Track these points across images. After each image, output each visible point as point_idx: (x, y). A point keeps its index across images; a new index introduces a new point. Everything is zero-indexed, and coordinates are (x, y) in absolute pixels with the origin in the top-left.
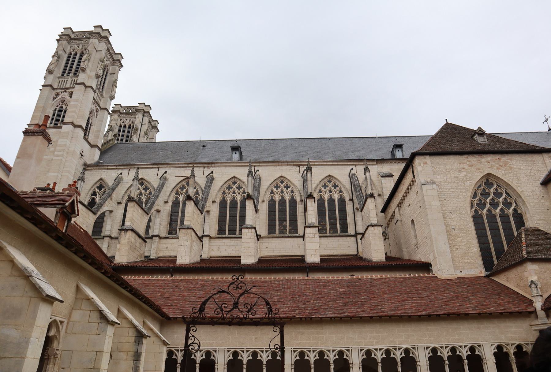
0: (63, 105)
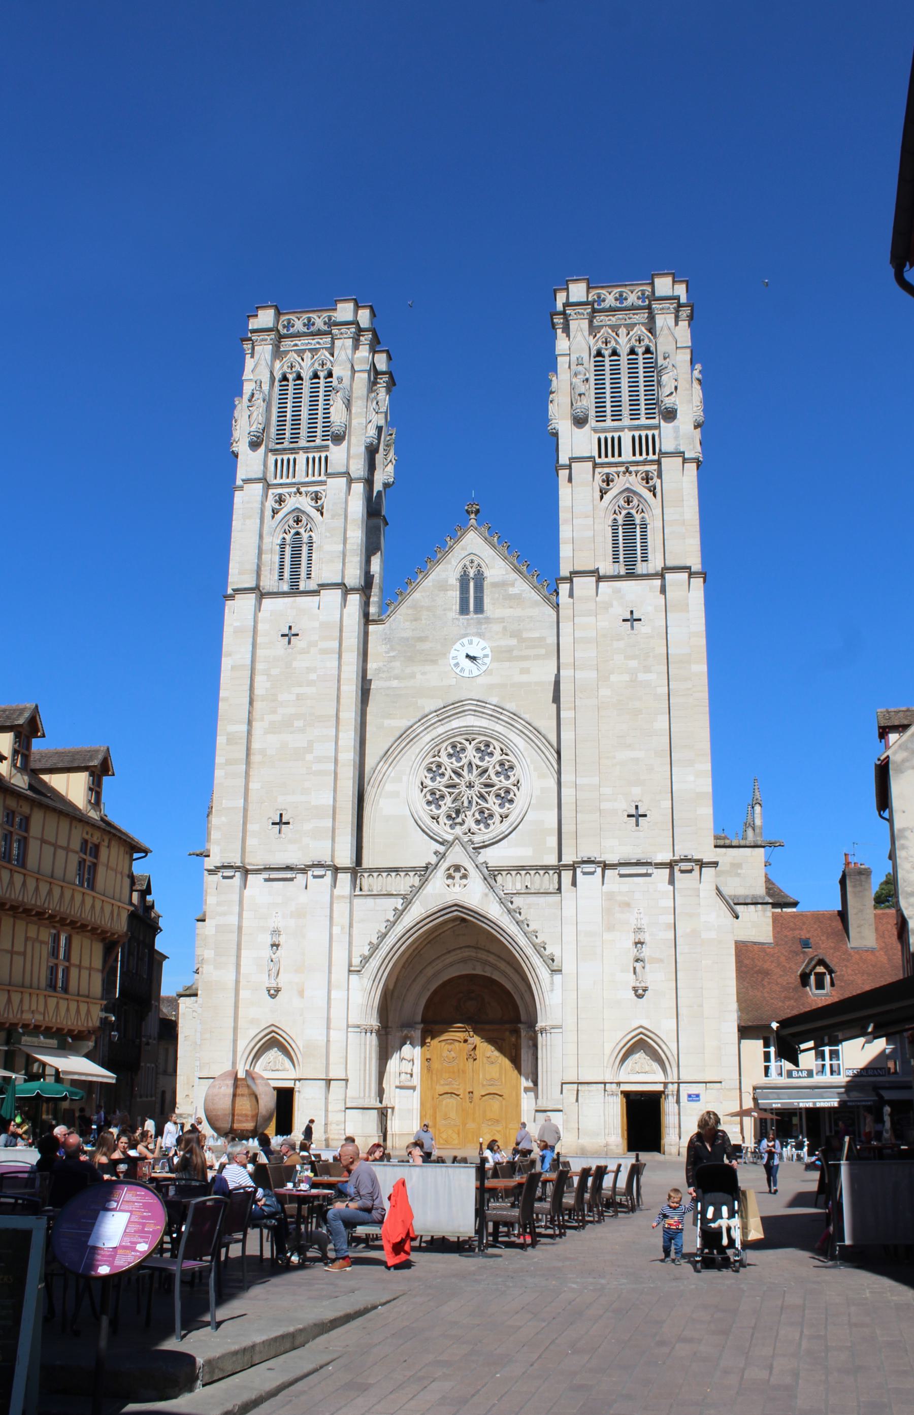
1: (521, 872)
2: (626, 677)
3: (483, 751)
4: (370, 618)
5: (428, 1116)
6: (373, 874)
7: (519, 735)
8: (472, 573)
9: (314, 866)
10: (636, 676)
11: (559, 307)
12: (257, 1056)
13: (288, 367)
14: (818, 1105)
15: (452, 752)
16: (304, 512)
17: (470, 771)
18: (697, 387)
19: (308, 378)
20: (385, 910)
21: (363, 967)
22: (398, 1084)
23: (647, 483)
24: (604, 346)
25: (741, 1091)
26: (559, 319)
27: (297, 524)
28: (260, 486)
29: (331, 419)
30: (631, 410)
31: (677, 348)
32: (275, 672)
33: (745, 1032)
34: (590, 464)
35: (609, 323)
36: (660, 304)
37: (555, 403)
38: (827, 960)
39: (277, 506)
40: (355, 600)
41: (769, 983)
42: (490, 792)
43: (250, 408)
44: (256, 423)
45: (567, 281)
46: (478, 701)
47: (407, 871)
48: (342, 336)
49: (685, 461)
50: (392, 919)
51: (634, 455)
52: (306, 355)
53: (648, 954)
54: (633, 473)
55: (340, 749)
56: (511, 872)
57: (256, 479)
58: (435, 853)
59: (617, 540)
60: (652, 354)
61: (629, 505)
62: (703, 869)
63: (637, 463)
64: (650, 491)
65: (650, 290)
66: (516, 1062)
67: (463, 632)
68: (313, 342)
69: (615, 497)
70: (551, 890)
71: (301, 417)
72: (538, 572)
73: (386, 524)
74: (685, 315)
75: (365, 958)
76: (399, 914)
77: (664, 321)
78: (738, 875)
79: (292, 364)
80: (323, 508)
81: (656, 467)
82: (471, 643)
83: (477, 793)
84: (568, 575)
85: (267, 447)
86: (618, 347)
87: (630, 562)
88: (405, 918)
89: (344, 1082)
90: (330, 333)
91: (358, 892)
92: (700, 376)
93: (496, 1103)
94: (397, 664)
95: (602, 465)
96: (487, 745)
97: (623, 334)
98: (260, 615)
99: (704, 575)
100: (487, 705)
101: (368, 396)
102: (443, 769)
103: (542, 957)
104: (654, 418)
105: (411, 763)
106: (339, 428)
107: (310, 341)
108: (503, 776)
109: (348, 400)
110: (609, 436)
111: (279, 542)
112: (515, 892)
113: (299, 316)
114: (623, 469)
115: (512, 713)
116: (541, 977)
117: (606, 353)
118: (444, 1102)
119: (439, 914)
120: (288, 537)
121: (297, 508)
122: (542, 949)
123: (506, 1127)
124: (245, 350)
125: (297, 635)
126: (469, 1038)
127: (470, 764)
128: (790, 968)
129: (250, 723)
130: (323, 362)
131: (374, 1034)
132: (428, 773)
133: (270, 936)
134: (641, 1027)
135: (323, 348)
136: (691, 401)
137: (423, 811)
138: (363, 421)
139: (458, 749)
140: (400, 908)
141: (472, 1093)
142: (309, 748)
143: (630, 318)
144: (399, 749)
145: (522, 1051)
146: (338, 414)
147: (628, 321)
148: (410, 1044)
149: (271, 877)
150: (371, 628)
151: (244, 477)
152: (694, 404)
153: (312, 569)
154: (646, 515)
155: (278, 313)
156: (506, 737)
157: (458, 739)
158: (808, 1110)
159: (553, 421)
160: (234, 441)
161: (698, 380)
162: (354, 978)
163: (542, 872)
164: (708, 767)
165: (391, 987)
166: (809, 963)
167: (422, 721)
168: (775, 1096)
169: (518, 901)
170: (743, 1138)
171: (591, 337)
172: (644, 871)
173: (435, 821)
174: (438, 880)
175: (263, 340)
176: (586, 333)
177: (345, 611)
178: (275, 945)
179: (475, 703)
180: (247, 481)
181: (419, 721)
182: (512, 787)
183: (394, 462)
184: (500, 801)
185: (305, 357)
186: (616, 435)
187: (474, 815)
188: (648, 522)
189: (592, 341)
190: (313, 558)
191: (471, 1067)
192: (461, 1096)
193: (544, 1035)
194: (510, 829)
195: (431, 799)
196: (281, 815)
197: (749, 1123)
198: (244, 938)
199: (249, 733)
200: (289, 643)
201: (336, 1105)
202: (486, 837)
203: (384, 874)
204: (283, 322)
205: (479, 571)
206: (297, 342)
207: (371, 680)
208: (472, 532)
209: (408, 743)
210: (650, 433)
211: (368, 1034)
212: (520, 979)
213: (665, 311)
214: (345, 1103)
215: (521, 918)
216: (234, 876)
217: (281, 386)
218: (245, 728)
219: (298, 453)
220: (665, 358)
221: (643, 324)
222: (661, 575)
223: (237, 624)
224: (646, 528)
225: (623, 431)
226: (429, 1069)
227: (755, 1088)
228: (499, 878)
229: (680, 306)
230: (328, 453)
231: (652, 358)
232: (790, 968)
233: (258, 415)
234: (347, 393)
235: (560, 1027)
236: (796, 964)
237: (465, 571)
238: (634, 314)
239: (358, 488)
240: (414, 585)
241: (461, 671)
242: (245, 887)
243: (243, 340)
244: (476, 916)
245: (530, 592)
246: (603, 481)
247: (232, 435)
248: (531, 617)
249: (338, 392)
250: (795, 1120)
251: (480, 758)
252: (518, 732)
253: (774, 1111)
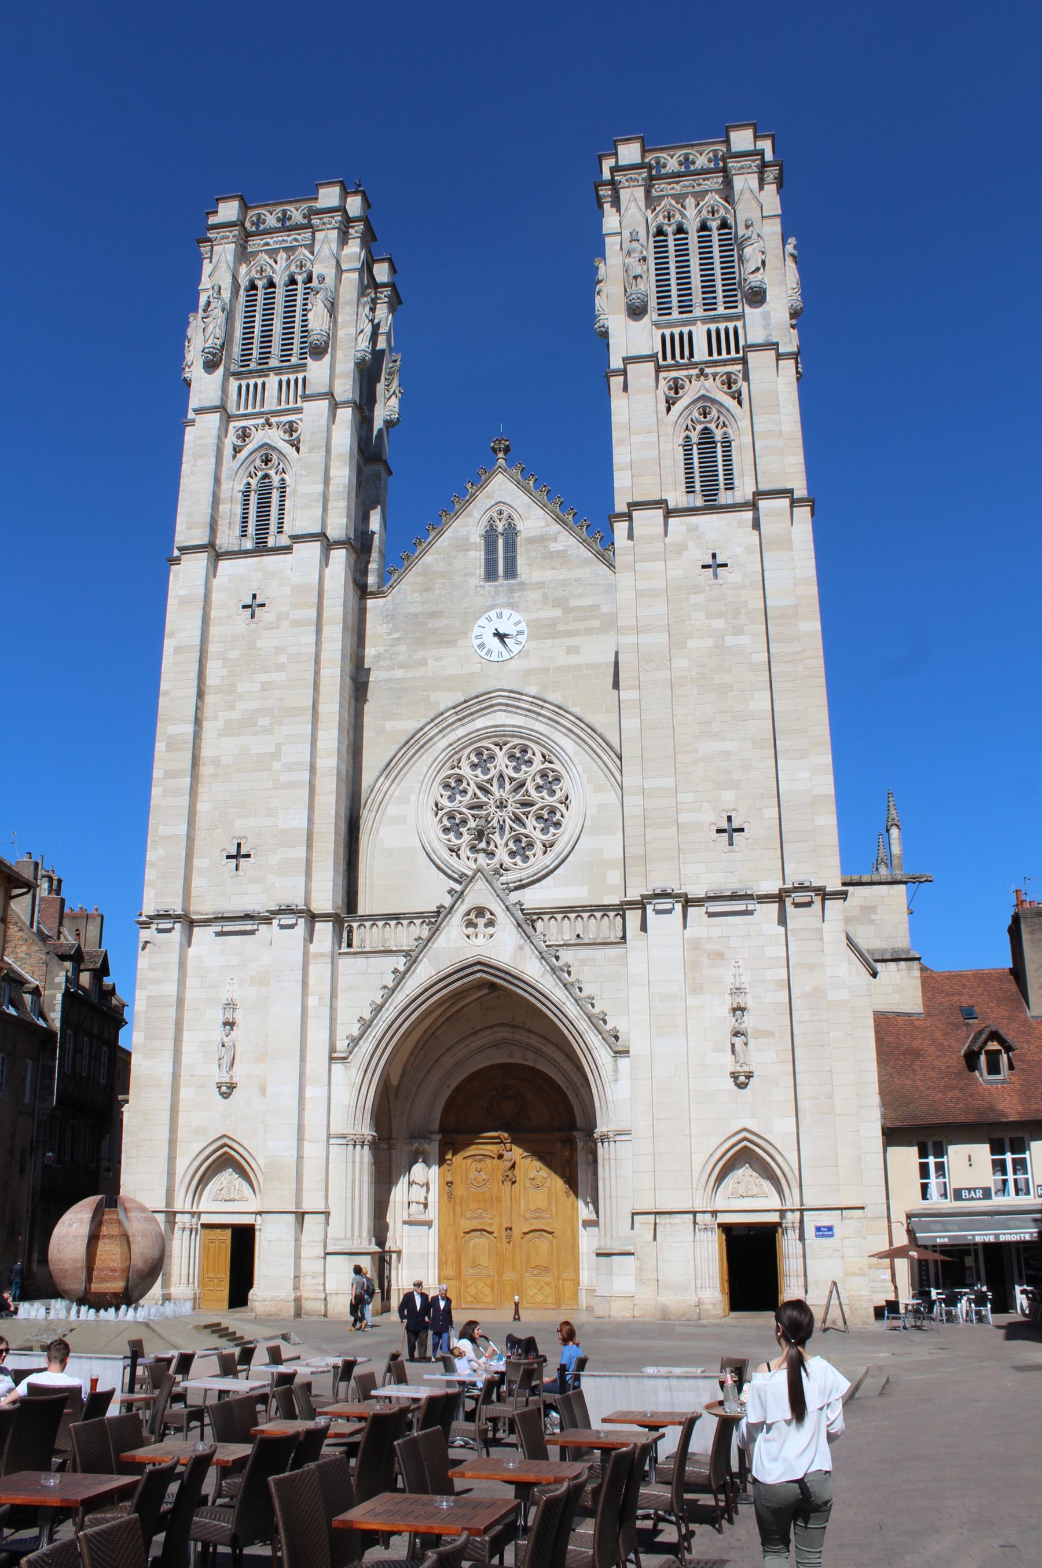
0: (709, 425)
1: (569, 915)
2: (710, 642)
3: (518, 758)
4: (369, 590)
5: (449, 1263)
6: (365, 923)
7: (566, 735)
8: (500, 527)
9: (280, 912)
10: (723, 639)
11: (606, 175)
12: (204, 1181)
13: (257, 272)
14: (1002, 1239)
15: (476, 761)
16: (274, 448)
17: (501, 786)
18: (791, 264)
19: (282, 283)
20: (382, 973)
21: (351, 1053)
22: (406, 1218)
23: (730, 388)
24: (666, 221)
25: (889, 1221)
26: (605, 190)
27: (266, 465)
28: (216, 416)
29: (309, 327)
30: (704, 299)
31: (763, 217)
32: (232, 655)
33: (892, 1136)
34: (651, 366)
35: (671, 192)
36: (739, 162)
37: (604, 294)
38: (1003, 1032)
39: (239, 443)
40: (339, 557)
41: (922, 1067)
43: (205, 320)
44: (212, 338)
45: (615, 141)
46: (510, 691)
47: (411, 917)
48: (324, 227)
49: (779, 357)
50: (391, 985)
51: (711, 354)
52: (279, 256)
53: (751, 1025)
54: (710, 376)
55: (319, 753)
56: (555, 915)
57: (211, 408)
58: (449, 892)
59: (692, 463)
60: (730, 228)
61: (705, 417)
62: (826, 902)
63: (715, 363)
64: (734, 398)
65: (725, 150)
66: (572, 1182)
67: (489, 603)
68: (289, 239)
69: (687, 408)
70: (612, 939)
71: (273, 333)
72: (589, 522)
73: (391, 473)
74: (772, 176)
75: (353, 1041)
76: (401, 977)
77: (744, 183)
78: (872, 922)
79: (261, 268)
80: (299, 442)
81: (740, 367)
82: (500, 616)
83: (511, 814)
84: (626, 510)
85: (227, 368)
86: (684, 221)
87: (710, 492)
88: (409, 983)
89: (323, 1216)
90: (309, 226)
91: (344, 949)
92: (795, 252)
93: (543, 1244)
94: (403, 648)
95: (668, 369)
96: (524, 751)
97: (690, 205)
98: (216, 582)
99: (811, 502)
100: (523, 697)
101: (359, 301)
102: (464, 785)
103: (600, 1033)
104: (736, 307)
105: (421, 778)
106: (319, 337)
107: (284, 238)
108: (545, 791)
109: (332, 304)
110: (676, 331)
111: (242, 488)
112: (562, 943)
113: (271, 208)
114: (694, 372)
115: (556, 706)
116: (599, 1062)
117: (670, 230)
118: (471, 1244)
119: (455, 977)
120: (254, 482)
121: (266, 444)
122: (601, 1022)
123: (559, 1278)
124: (202, 254)
125: (263, 605)
126: (505, 1153)
127: (501, 776)
128: (950, 1046)
129: (198, 722)
130: (301, 263)
131: (366, 1148)
132: (445, 790)
133: (222, 1011)
134: (745, 1130)
135: (301, 246)
136: (784, 282)
137: (438, 841)
138: (353, 331)
139: (485, 757)
140: (402, 968)
141: (510, 1229)
142: (276, 755)
143: (699, 185)
144: (406, 760)
145: (579, 1168)
146: (318, 320)
147: (697, 189)
148: (424, 1161)
149: (225, 929)
150: (370, 603)
151: (196, 407)
152: (789, 286)
153: (285, 521)
154: (729, 430)
155: (245, 207)
156: (549, 738)
157: (484, 743)
158: (986, 1245)
159: (602, 317)
160: (187, 365)
161: (792, 255)
162: (337, 1067)
163: (598, 915)
164: (828, 759)
165: (395, 1081)
166: (975, 1039)
167: (436, 722)
168: (939, 1227)
169: (567, 956)
170: (896, 1288)
171: (649, 211)
172: (743, 908)
173: (454, 854)
174: (453, 930)
175: (223, 238)
176: (642, 204)
177: (327, 571)
178: (230, 1024)
179: (507, 694)
180: (199, 411)
181: (432, 721)
182: (558, 805)
183: (399, 395)
184: (542, 825)
185: (279, 259)
186: (685, 330)
187: (507, 845)
188: (732, 437)
189: (650, 216)
190: (286, 507)
191: (508, 1193)
192: (495, 1235)
193: (606, 1144)
194: (557, 862)
195: (449, 825)
196: (239, 845)
197: (902, 1266)
198: (187, 1015)
199: (197, 735)
200: (253, 616)
201: (312, 1248)
202: (524, 874)
203: (381, 924)
204: (251, 217)
205: (510, 524)
206: (268, 240)
207: (369, 670)
208: (500, 475)
209: (417, 751)
210: (731, 326)
211: (358, 1147)
212: (575, 1069)
213: (745, 171)
214: (325, 1246)
215: (570, 979)
216: (173, 928)
217: (247, 296)
218: (190, 728)
219: (267, 376)
220: (747, 227)
221: (717, 191)
222: (753, 506)
223: (182, 592)
224: (730, 446)
225: (694, 324)
226: (450, 1196)
227: (909, 1216)
228: (539, 925)
229: (764, 165)
230: (305, 374)
231: (730, 234)
232: (950, 1046)
233: (215, 328)
234: (330, 293)
235: (627, 1133)
236: (957, 1040)
237: (491, 525)
238: (704, 179)
239: (346, 415)
240: (424, 545)
241: (487, 654)
242: (189, 945)
243: (199, 241)
244: (508, 977)
245: (578, 547)
246: (670, 389)
247: (184, 358)
248: (580, 579)
249: (317, 293)
250: (969, 1261)
251: (514, 768)
253: (938, 1249)
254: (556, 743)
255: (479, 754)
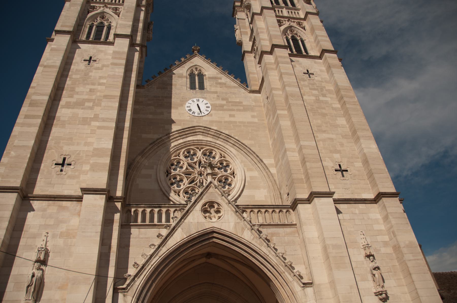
2: (314, 98)
10: (319, 98)
42: (216, 178)
82: (198, 101)
96: (211, 153)
179: (203, 128)
245: (231, 82)
252: (232, 145)
254: (228, 149)
255: (189, 152)
